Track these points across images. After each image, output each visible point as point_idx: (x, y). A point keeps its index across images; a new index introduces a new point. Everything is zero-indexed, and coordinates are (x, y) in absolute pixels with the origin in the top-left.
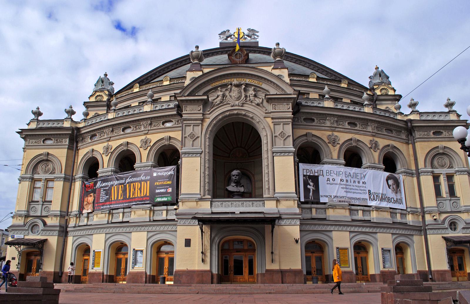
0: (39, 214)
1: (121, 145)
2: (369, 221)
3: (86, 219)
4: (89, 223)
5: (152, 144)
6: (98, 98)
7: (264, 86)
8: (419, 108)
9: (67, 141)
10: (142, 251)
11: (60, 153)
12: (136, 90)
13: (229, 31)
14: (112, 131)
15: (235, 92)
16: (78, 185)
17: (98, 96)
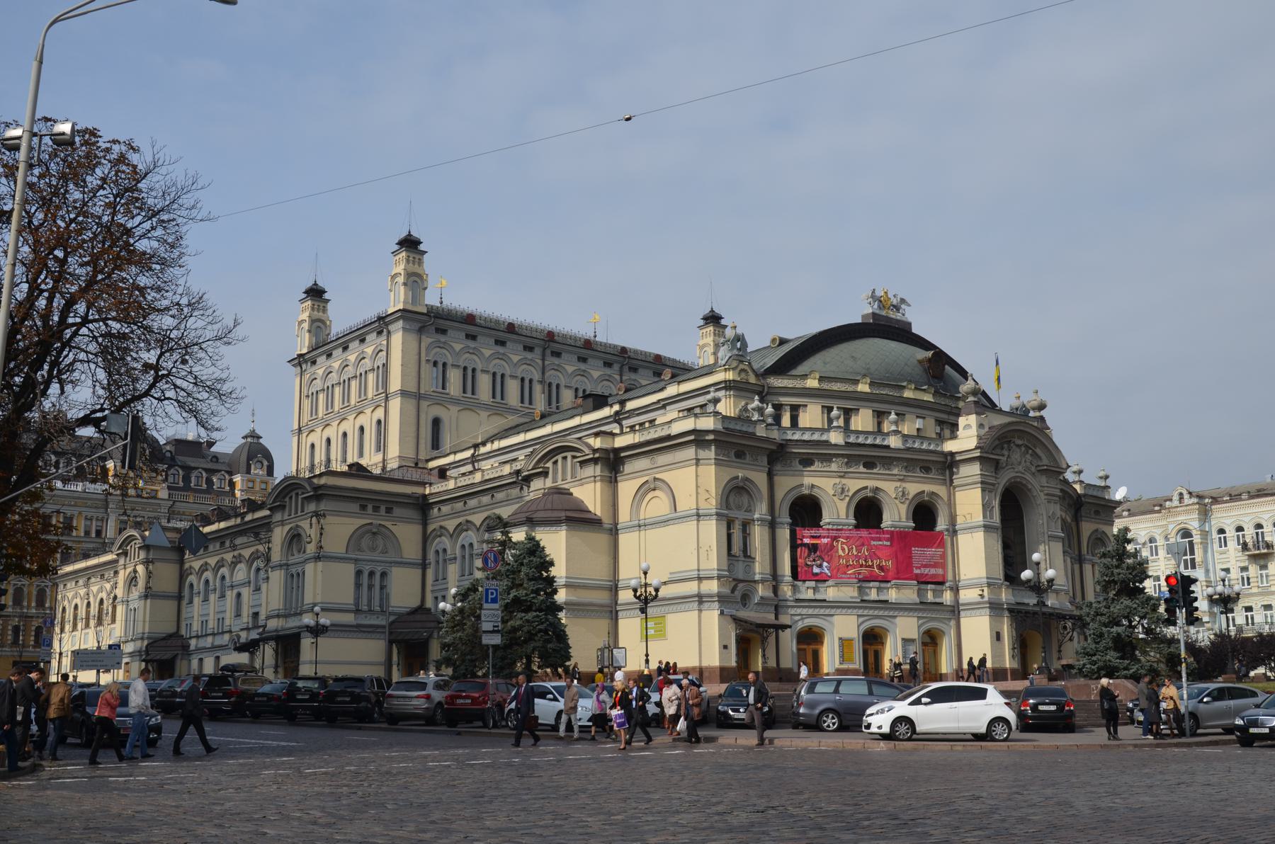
0: (741, 577)
1: (866, 488)
2: (886, 601)
3: (810, 592)
4: (818, 597)
5: (910, 497)
6: (743, 375)
7: (1038, 451)
8: (1083, 477)
9: (765, 459)
10: (913, 641)
11: (760, 479)
12: (812, 383)
13: (874, 291)
14: (847, 464)
15: (1016, 456)
16: (784, 534)
17: (742, 370)
